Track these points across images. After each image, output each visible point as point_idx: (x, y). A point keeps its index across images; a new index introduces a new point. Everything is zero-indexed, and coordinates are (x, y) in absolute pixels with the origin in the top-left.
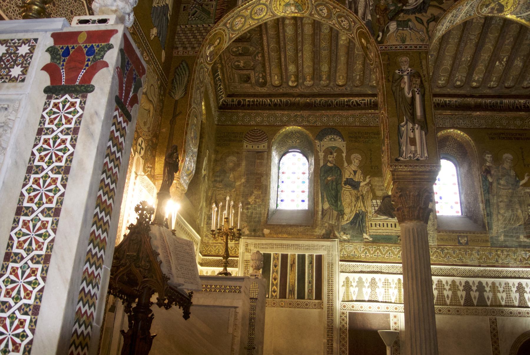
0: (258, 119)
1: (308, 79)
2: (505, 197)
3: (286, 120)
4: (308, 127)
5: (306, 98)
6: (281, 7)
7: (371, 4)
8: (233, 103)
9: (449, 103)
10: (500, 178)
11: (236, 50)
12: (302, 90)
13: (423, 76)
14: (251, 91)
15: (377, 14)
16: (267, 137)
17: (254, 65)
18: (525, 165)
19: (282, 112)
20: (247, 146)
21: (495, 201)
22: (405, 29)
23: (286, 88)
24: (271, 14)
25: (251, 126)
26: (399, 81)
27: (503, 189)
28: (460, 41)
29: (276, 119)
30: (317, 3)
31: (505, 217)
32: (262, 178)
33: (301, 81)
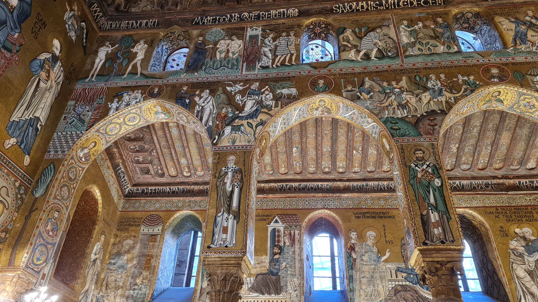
0: (157, 205)
1: (200, 170)
2: (367, 273)
4: (199, 211)
5: (199, 186)
6: (152, 115)
7: (214, 112)
9: (321, 187)
12: (196, 179)
13: (243, 172)
14: (153, 181)
17: (151, 159)
18: (386, 242)
19: (178, 198)
20: (144, 230)
21: (358, 277)
23: (181, 177)
26: (223, 177)
27: (365, 265)
28: (316, 136)
29: (173, 205)
30: (177, 112)
31: (366, 293)
33: (193, 172)
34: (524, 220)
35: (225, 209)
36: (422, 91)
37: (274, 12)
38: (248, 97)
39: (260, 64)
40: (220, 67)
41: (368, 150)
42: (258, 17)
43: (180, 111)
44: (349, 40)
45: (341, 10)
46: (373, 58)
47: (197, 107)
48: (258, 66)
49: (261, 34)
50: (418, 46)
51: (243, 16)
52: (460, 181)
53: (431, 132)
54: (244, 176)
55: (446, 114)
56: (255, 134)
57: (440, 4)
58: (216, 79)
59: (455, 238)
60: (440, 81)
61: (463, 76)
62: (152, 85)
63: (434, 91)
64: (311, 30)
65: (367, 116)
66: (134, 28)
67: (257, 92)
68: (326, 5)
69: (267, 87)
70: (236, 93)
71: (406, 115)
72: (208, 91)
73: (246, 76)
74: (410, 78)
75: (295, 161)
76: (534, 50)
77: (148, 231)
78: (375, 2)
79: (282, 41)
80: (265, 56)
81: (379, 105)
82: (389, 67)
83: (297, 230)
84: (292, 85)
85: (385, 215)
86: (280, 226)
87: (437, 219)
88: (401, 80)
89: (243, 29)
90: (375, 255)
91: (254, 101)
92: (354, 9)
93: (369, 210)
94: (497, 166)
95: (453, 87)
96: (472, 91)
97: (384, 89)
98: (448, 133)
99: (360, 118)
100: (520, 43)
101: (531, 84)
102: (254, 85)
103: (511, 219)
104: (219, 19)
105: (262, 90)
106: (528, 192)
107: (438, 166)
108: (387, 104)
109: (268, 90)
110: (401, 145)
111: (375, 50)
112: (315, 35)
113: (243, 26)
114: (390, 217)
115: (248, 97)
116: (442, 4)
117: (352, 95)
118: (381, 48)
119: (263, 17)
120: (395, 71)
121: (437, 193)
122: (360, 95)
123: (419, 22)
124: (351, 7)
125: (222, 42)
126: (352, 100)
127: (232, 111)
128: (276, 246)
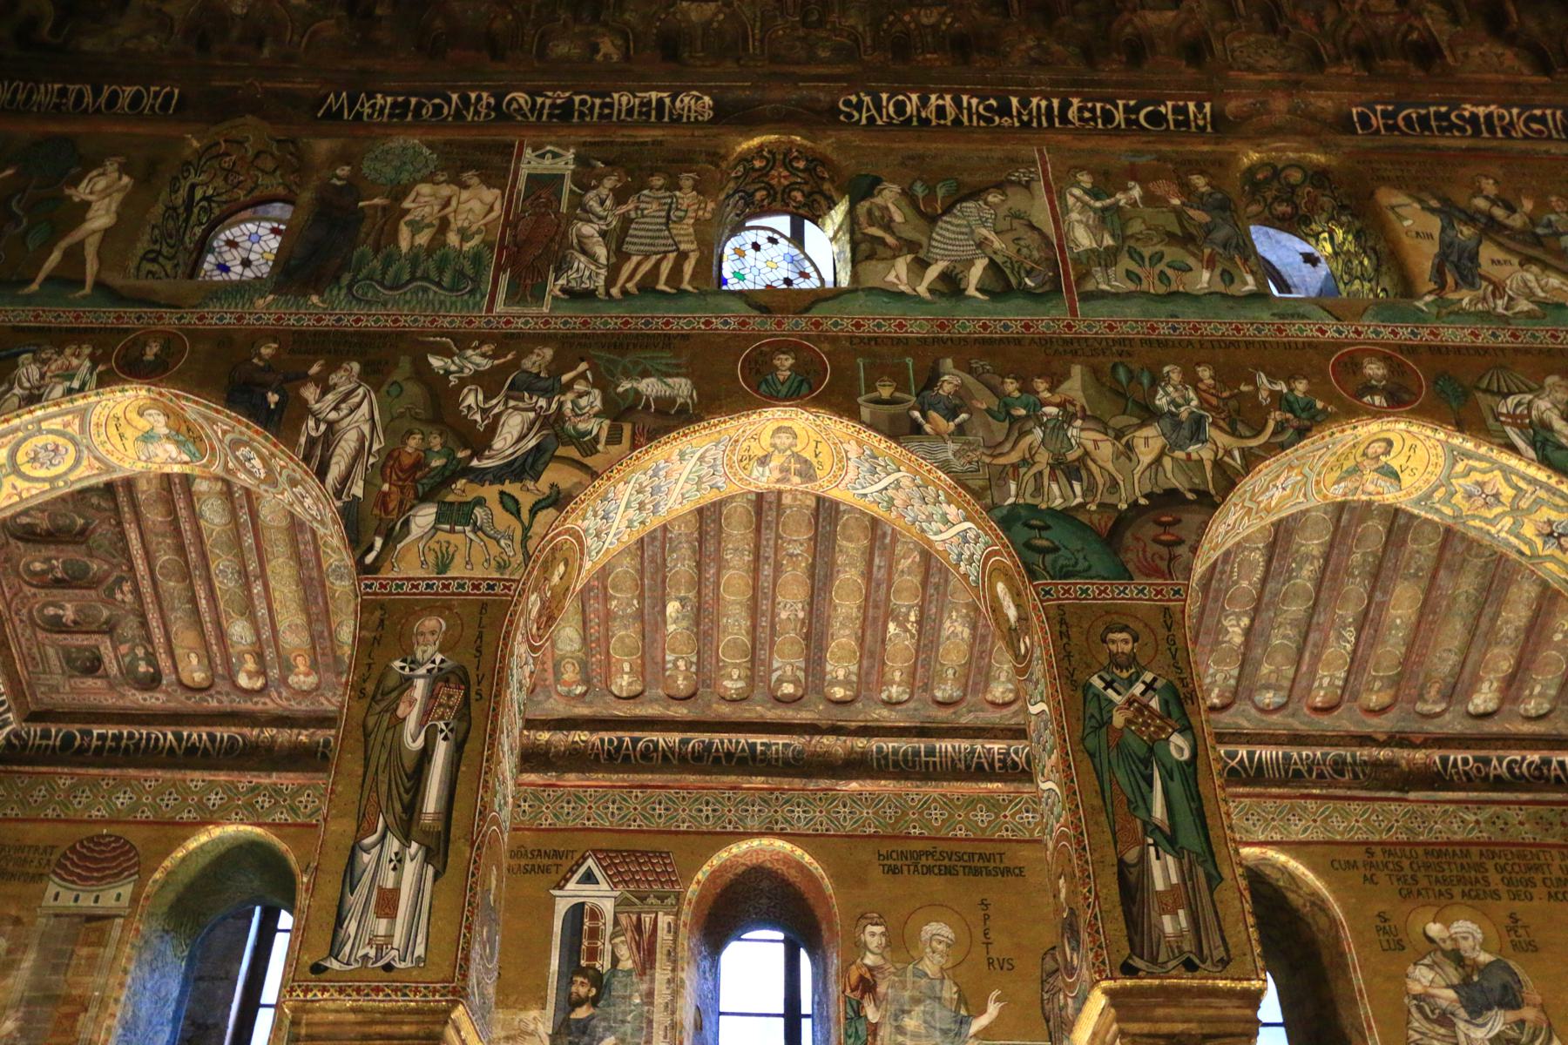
0: (122, 800)
1: (302, 668)
3: (218, 802)
4: (287, 830)
5: (296, 731)
6: (129, 444)
7: (375, 447)
8: (44, 742)
9: (763, 753)
10: (906, 1008)
11: (45, 567)
12: (285, 703)
13: (473, 679)
14: (110, 701)
15: (384, 481)
16: (138, 864)
18: (990, 963)
19: (208, 776)
20: (60, 895)
22: (458, 528)
23: (228, 694)
24: (97, 464)
25: (92, 822)
26: (394, 695)
29: (185, 799)
30: (229, 437)
32: (82, 1016)
33: (274, 673)
34: (1457, 891)
35: (391, 819)
36: (1135, 421)
37: (624, 100)
38: (508, 398)
39: (562, 282)
40: (409, 282)
41: (941, 623)
42: (564, 112)
43: (241, 433)
44: (891, 220)
45: (864, 115)
46: (971, 291)
47: (311, 423)
48: (555, 286)
49: (574, 172)
50: (1126, 263)
51: (509, 104)
52: (1251, 748)
53: (1163, 565)
54: (473, 695)
55: (1215, 506)
56: (525, 538)
57: (1202, 130)
58: (390, 323)
59: (1233, 951)
60: (1196, 389)
61: (1273, 378)
62: (134, 330)
63: (1177, 424)
64: (755, 175)
65: (942, 498)
66: (86, 110)
67: (542, 384)
68: (814, 93)
69: (583, 366)
70: (463, 382)
71: (1079, 500)
72: (356, 366)
73: (508, 322)
74: (1095, 372)
75: (673, 651)
76: (1500, 310)
77: (76, 899)
78: (983, 99)
79: (650, 205)
80: (584, 252)
81: (987, 460)
82: (1027, 327)
83: (666, 914)
84: (678, 366)
85: (992, 865)
86: (603, 897)
87: (1174, 880)
88: (1066, 375)
89: (507, 151)
90: (946, 1013)
91: (532, 415)
92: (911, 116)
93: (934, 843)
94: (1374, 700)
95: (1238, 412)
96: (1302, 433)
97: (1006, 405)
98: (1217, 575)
99: (917, 503)
100: (1457, 284)
101: (1491, 421)
102: (534, 358)
103: (1414, 889)
104: (420, 106)
105: (565, 378)
106: (1473, 795)
107: (1182, 691)
108: (1014, 457)
109: (586, 379)
110: (1059, 606)
111: (979, 267)
112: (769, 195)
113: (508, 138)
114: (1007, 871)
115: (508, 398)
116: (1209, 129)
117: (893, 419)
118: (999, 259)
119: (582, 115)
120: (1045, 342)
121: (1176, 787)
122: (921, 420)
123: (1131, 184)
124: (900, 108)
125: (425, 189)
126: (893, 435)
127: (443, 445)
128: (581, 971)
